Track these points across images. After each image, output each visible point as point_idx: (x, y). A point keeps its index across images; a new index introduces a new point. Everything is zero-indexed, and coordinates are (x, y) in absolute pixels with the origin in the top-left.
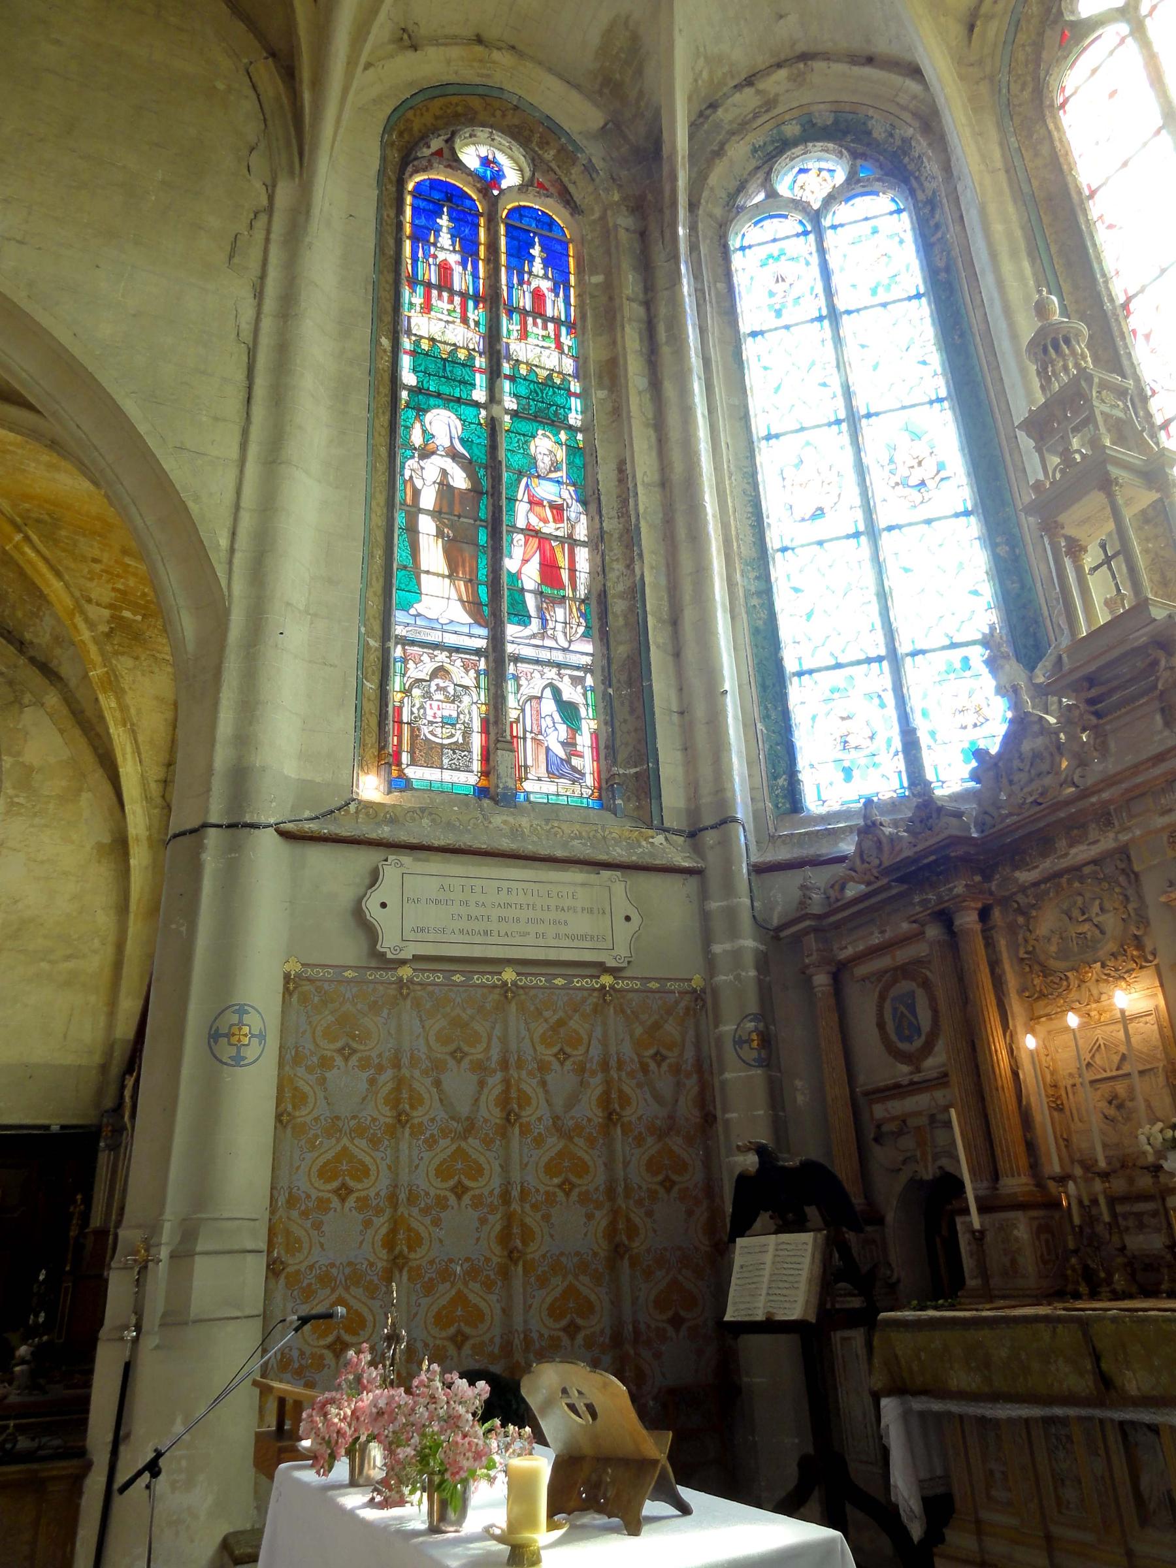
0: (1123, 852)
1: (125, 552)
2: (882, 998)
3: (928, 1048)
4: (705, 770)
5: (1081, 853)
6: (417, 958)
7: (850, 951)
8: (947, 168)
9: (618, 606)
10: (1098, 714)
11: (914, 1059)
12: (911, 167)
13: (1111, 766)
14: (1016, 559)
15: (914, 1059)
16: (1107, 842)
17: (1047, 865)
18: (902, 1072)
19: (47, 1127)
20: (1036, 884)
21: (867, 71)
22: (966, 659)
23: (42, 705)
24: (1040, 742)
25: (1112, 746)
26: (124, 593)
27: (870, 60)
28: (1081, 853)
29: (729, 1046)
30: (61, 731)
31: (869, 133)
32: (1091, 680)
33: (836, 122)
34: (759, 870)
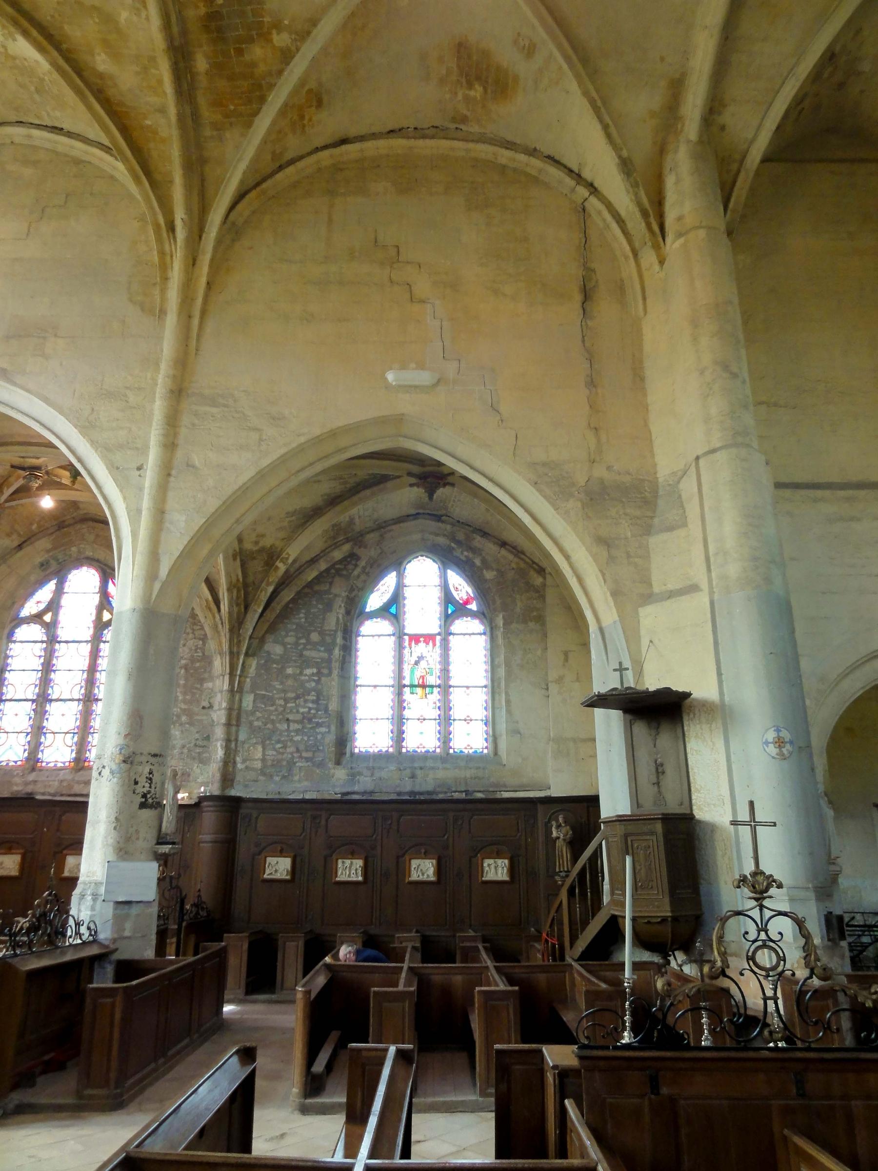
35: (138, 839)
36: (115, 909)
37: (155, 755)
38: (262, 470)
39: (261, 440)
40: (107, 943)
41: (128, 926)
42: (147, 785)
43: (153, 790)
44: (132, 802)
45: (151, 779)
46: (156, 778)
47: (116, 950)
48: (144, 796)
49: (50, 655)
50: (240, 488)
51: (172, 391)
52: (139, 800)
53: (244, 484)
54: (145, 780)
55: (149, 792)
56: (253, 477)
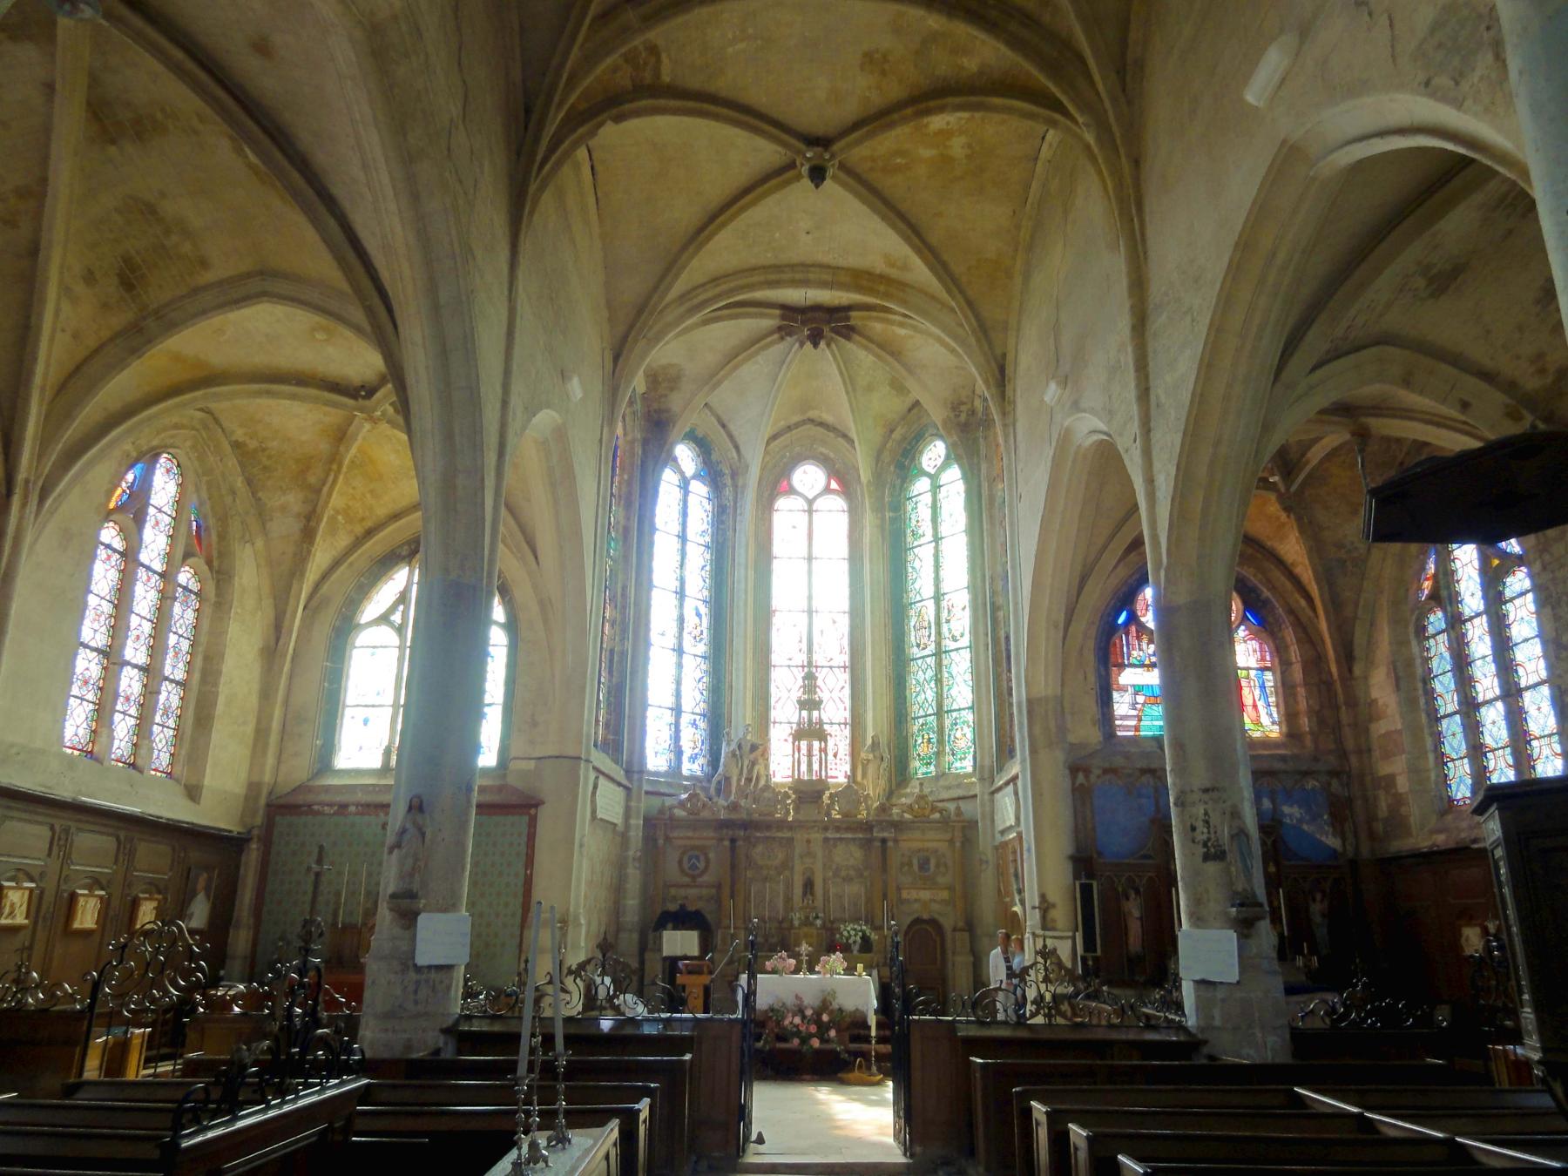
0: (792, 839)
1: (372, 491)
2: (684, 853)
3: (701, 875)
4: (637, 747)
5: (780, 834)
6: (601, 820)
7: (675, 834)
8: (735, 503)
9: (616, 658)
10: (800, 802)
11: (693, 877)
12: (720, 484)
13: (801, 817)
14: (719, 688)
15: (693, 877)
16: (788, 834)
17: (768, 834)
18: (686, 880)
19: (230, 831)
20: (759, 838)
21: (722, 431)
22: (695, 720)
23: (253, 544)
24: (771, 795)
25: (802, 812)
26: (349, 507)
27: (724, 426)
28: (780, 834)
29: (630, 860)
30: (258, 566)
31: (710, 454)
32: (801, 792)
33: (701, 439)
34: (647, 793)
35: (1209, 900)
36: (1196, 991)
37: (1206, 791)
38: (1202, 359)
39: (1193, 321)
40: (1194, 1031)
41: (1217, 1013)
42: (1205, 830)
43: (1213, 836)
44: (1193, 854)
45: (1207, 822)
46: (1215, 819)
47: (1205, 1042)
48: (1205, 845)
49: (1459, 645)
50: (1192, 402)
51: (1134, 328)
52: (1201, 850)
53: (1193, 394)
54: (1201, 823)
55: (1209, 839)
56: (1197, 378)
